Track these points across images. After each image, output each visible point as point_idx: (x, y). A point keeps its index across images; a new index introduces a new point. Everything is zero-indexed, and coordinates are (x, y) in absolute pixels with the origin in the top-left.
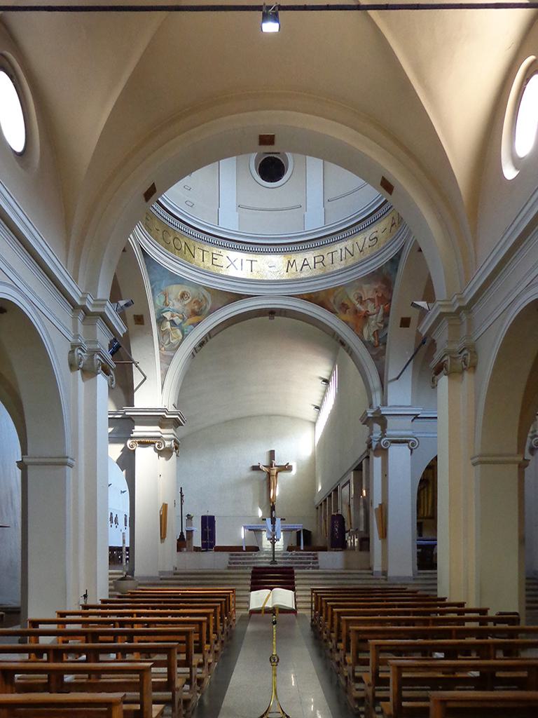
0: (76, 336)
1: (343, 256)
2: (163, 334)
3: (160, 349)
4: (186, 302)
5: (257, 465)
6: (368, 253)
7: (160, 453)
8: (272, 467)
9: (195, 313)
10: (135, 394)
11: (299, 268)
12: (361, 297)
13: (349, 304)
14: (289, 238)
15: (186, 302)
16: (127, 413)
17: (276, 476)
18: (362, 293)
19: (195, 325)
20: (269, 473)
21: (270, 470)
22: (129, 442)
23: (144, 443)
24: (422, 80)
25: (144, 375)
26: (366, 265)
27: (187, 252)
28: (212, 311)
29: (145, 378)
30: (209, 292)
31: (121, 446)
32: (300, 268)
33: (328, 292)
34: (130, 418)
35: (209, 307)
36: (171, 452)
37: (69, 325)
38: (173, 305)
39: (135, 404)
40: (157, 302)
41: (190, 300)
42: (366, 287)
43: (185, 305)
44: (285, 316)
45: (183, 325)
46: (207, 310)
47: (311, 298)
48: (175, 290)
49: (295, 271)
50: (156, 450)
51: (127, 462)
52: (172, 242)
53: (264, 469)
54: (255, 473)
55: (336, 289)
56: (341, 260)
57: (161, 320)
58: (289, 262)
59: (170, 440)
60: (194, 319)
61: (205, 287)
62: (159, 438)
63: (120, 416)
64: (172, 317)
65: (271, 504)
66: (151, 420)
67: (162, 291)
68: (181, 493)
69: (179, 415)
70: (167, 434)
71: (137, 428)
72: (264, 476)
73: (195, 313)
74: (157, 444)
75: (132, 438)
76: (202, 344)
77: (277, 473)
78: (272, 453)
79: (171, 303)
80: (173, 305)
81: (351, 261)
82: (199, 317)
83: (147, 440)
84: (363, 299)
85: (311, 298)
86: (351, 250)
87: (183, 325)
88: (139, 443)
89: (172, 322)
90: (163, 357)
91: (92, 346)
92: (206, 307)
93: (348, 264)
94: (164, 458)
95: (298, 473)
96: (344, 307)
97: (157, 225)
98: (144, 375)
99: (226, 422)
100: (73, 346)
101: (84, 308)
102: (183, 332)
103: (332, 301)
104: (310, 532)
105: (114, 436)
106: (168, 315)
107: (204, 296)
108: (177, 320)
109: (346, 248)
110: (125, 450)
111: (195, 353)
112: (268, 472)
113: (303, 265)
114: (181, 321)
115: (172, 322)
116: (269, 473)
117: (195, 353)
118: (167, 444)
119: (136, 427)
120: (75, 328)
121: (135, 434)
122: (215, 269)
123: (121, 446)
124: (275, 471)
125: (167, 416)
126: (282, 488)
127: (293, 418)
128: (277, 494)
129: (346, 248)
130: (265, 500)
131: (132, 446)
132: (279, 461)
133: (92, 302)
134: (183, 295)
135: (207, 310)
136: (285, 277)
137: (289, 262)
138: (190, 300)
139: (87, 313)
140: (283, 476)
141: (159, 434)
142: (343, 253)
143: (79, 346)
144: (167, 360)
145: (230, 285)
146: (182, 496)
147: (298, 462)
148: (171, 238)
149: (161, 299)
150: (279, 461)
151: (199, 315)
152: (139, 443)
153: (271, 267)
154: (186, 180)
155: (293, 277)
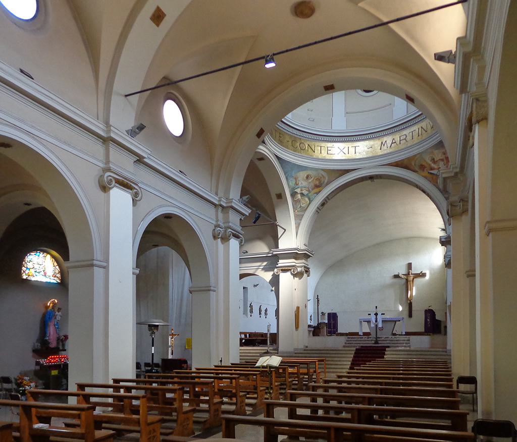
0: (217, 221)
1: (420, 133)
2: (295, 202)
3: (294, 212)
4: (310, 181)
5: (397, 274)
6: (416, 140)
7: (295, 275)
8: (409, 274)
9: (317, 186)
10: (279, 241)
11: (389, 145)
12: (434, 159)
13: (426, 165)
14: (381, 127)
15: (310, 181)
16: (274, 253)
17: (413, 281)
18: (434, 156)
19: (317, 193)
20: (407, 280)
21: (407, 277)
22: (276, 270)
23: (285, 270)
24: (417, 41)
25: (284, 229)
26: (435, 137)
27: (310, 150)
28: (329, 183)
29: (285, 231)
30: (325, 172)
31: (272, 273)
32: (390, 145)
33: (409, 159)
34: (276, 255)
35: (326, 181)
36: (303, 275)
37: (214, 217)
38: (302, 183)
39: (279, 247)
40: (290, 184)
41: (312, 179)
42: (436, 152)
43: (310, 183)
44: (381, 178)
45: (309, 195)
46: (325, 183)
47: (397, 165)
48: (302, 175)
49: (386, 148)
50: (292, 274)
51: (275, 281)
52: (299, 146)
53: (403, 276)
54: (397, 280)
55: (415, 156)
56: (419, 136)
57: (293, 194)
58: (382, 143)
59: (301, 267)
60: (316, 190)
61: (323, 170)
62: (293, 266)
63: (270, 255)
64: (301, 190)
65: (409, 302)
66: (292, 255)
67: (292, 177)
68: (318, 298)
69: (307, 251)
70: (299, 264)
71: (281, 261)
72: (404, 281)
73: (317, 186)
74: (292, 270)
75: (277, 268)
76: (323, 204)
77: (413, 279)
78: (410, 266)
79: (300, 183)
80: (302, 183)
81: (425, 136)
82: (319, 188)
83: (286, 268)
84: (436, 160)
85: (397, 165)
86: (425, 128)
87: (309, 195)
88: (282, 270)
89: (302, 194)
90: (296, 216)
91: (226, 225)
92: (324, 182)
93: (423, 138)
94: (298, 278)
95: (430, 278)
96: (422, 167)
97: (288, 138)
98: (284, 229)
99: (374, 245)
100: (216, 226)
101: (221, 205)
102: (309, 199)
103: (413, 164)
104: (440, 321)
105: (267, 267)
106: (298, 191)
107: (322, 175)
108: (305, 192)
109: (422, 127)
110: (274, 275)
111: (319, 211)
112: (407, 279)
113: (392, 143)
114: (307, 192)
115: (302, 194)
116: (407, 280)
117: (319, 211)
118: (299, 269)
119: (280, 261)
120: (217, 217)
121: (279, 265)
122: (328, 157)
123: (272, 273)
124: (412, 278)
125: (299, 252)
126: (417, 290)
127: (427, 238)
128: (414, 294)
129: (422, 127)
130: (404, 299)
131: (277, 273)
132: (415, 270)
133: (225, 201)
134: (307, 177)
135: (325, 183)
136: (380, 153)
137: (382, 143)
138: (312, 179)
139: (223, 207)
140: (418, 281)
141: (294, 264)
142: (420, 129)
143: (218, 226)
144: (299, 218)
145: (336, 165)
146: (318, 301)
147: (431, 270)
148: (298, 144)
149: (292, 183)
150: (415, 270)
151: (320, 187)
152: (282, 270)
153: (362, 149)
154: (308, 105)
155: (386, 152)
